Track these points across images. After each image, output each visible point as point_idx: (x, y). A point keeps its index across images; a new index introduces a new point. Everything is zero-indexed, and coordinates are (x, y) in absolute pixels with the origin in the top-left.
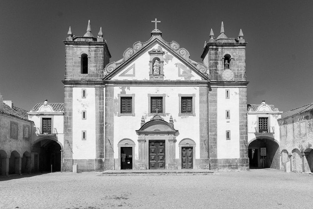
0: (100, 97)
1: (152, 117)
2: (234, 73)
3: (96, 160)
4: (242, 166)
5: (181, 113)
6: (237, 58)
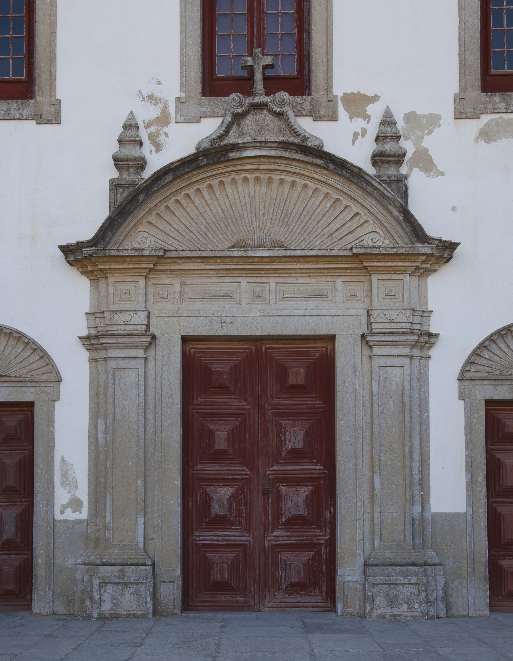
1: (209, 127)
5: (475, 93)
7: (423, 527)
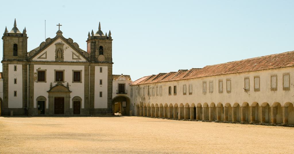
0: (25, 70)
1: (56, 83)
2: (105, 57)
3: (22, 108)
4: (109, 112)
5: (73, 81)
6: (107, 48)
7: (69, 109)
